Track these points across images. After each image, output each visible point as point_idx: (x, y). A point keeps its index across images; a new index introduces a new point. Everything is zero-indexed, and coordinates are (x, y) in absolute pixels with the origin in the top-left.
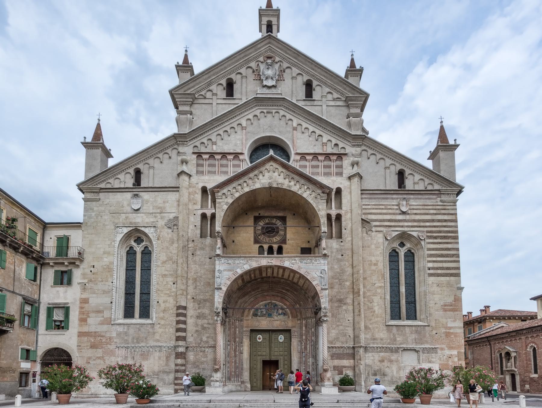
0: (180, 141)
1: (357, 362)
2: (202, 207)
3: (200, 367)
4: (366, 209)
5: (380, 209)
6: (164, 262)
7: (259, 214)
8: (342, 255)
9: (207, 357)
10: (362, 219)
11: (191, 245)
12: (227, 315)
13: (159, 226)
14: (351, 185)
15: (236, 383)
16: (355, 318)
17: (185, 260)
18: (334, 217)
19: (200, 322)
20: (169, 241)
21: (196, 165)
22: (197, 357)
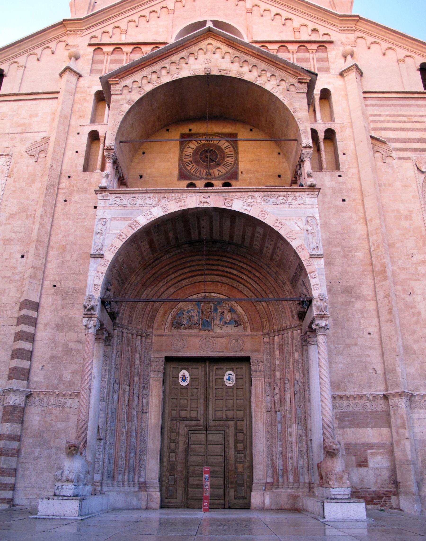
0: (71, 31)
1: (397, 432)
2: (93, 121)
3: (52, 443)
4: (375, 122)
5: (400, 122)
6: (12, 216)
7: (190, 130)
8: (344, 200)
9: (67, 419)
10: (372, 137)
11: (65, 184)
12: (117, 321)
13: (14, 154)
14: (345, 85)
15: (127, 488)
16: (383, 329)
17: (48, 209)
18: (321, 135)
19: (61, 337)
20: (28, 179)
21: (91, 62)
22: (48, 419)
